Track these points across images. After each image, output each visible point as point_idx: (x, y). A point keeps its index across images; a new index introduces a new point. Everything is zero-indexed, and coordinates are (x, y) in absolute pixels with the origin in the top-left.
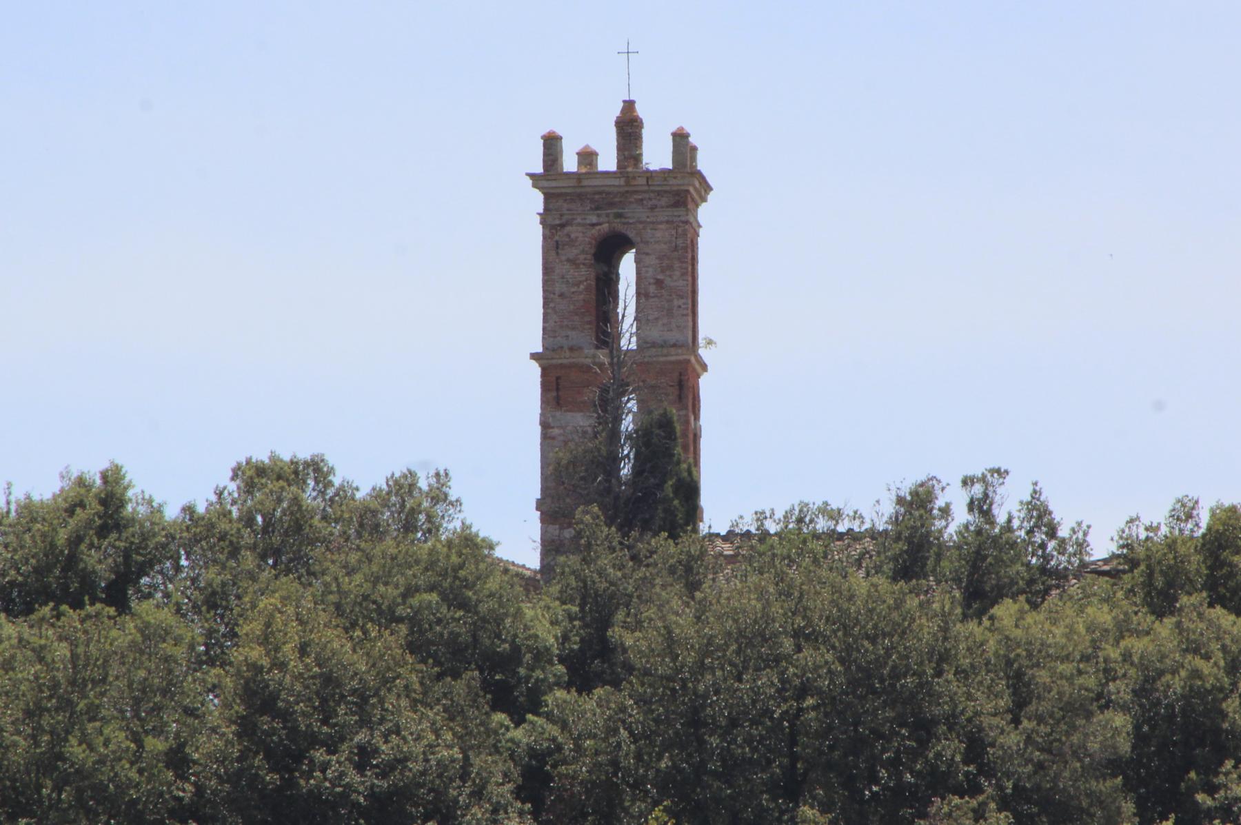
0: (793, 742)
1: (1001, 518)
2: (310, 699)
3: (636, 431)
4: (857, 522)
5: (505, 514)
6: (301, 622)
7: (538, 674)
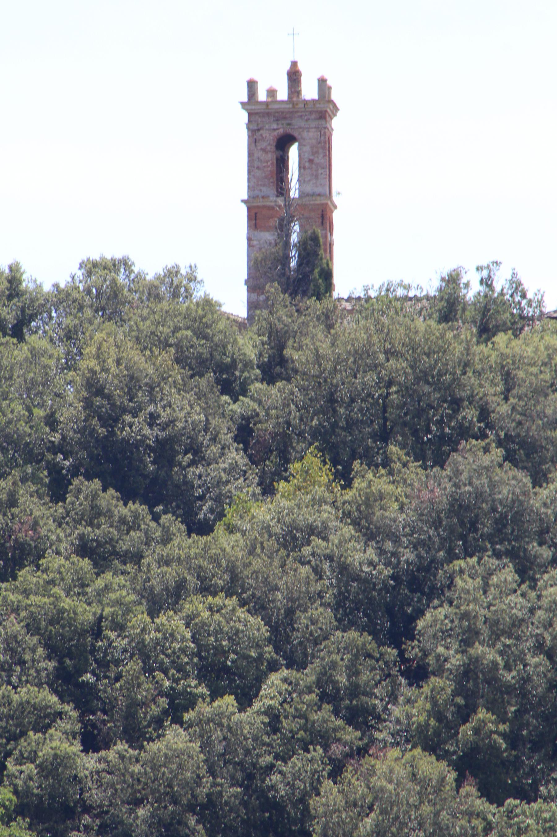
0: (385, 411)
1: (498, 289)
2: (122, 388)
3: (299, 242)
4: (419, 291)
5: (227, 288)
6: (117, 347)
7: (246, 374)
